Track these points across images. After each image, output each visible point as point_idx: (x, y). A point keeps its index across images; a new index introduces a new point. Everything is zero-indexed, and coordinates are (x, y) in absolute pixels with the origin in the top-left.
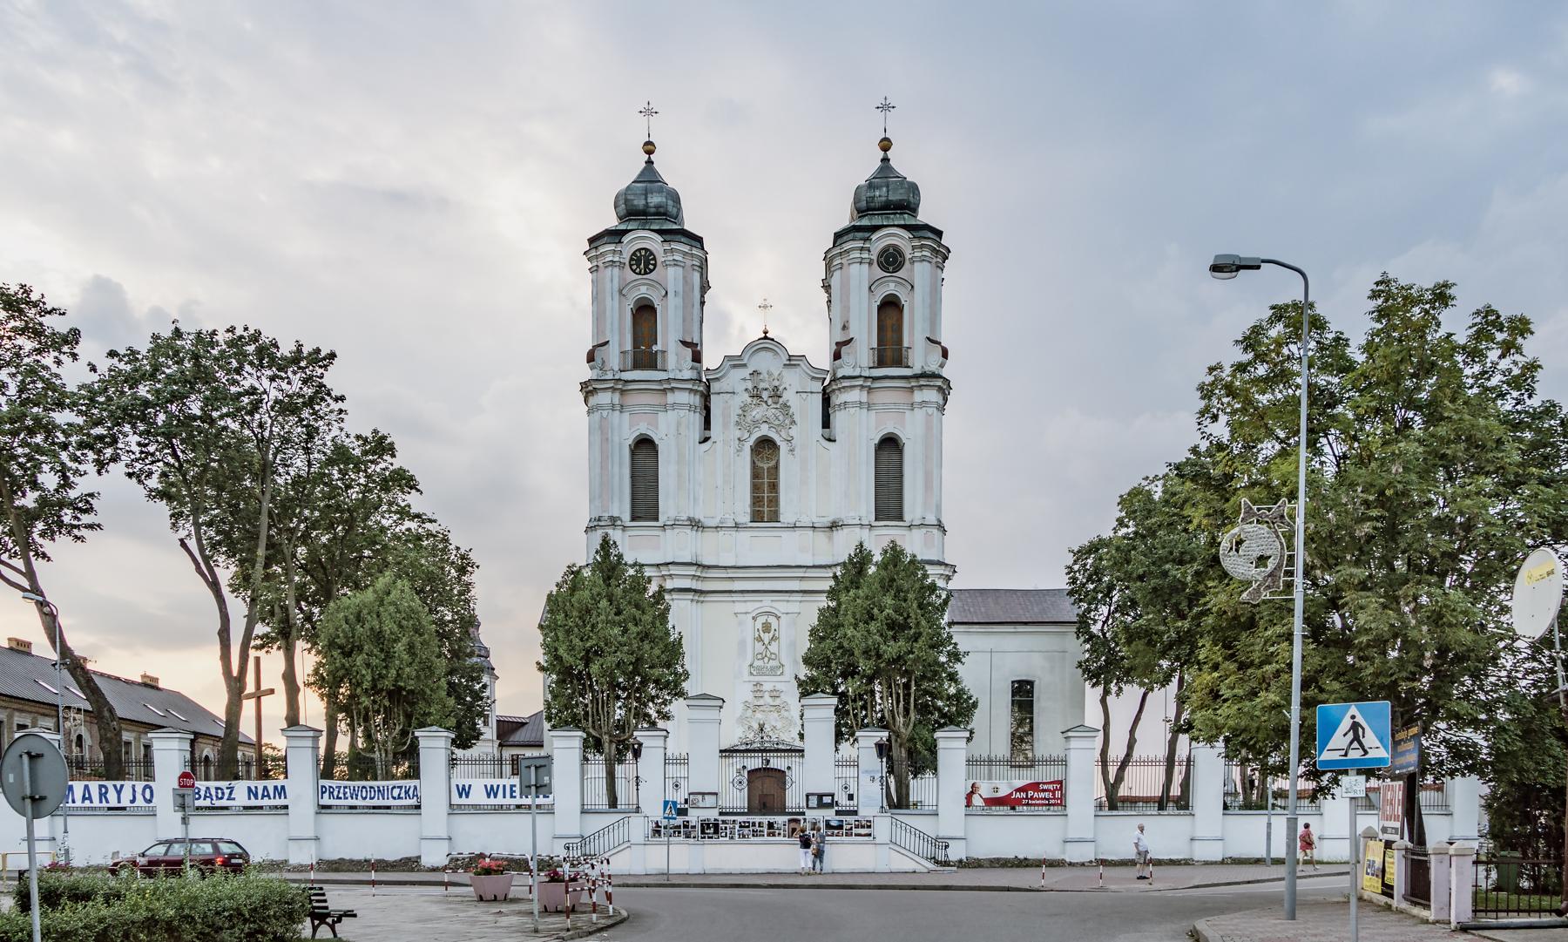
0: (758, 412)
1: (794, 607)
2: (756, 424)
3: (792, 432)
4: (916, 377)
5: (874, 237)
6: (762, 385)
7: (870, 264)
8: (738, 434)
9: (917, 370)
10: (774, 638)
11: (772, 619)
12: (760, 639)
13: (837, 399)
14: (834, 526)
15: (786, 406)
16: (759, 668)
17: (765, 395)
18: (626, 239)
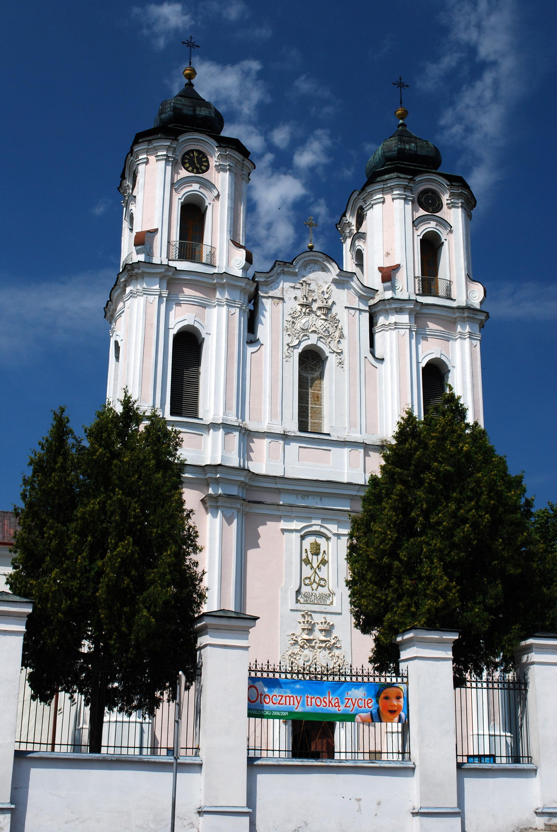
3: (340, 346)
4: (459, 308)
5: (418, 179)
7: (413, 202)
8: (287, 340)
10: (324, 562)
11: (321, 541)
12: (308, 562)
13: (381, 320)
16: (306, 596)
17: (315, 306)
18: (182, 138)
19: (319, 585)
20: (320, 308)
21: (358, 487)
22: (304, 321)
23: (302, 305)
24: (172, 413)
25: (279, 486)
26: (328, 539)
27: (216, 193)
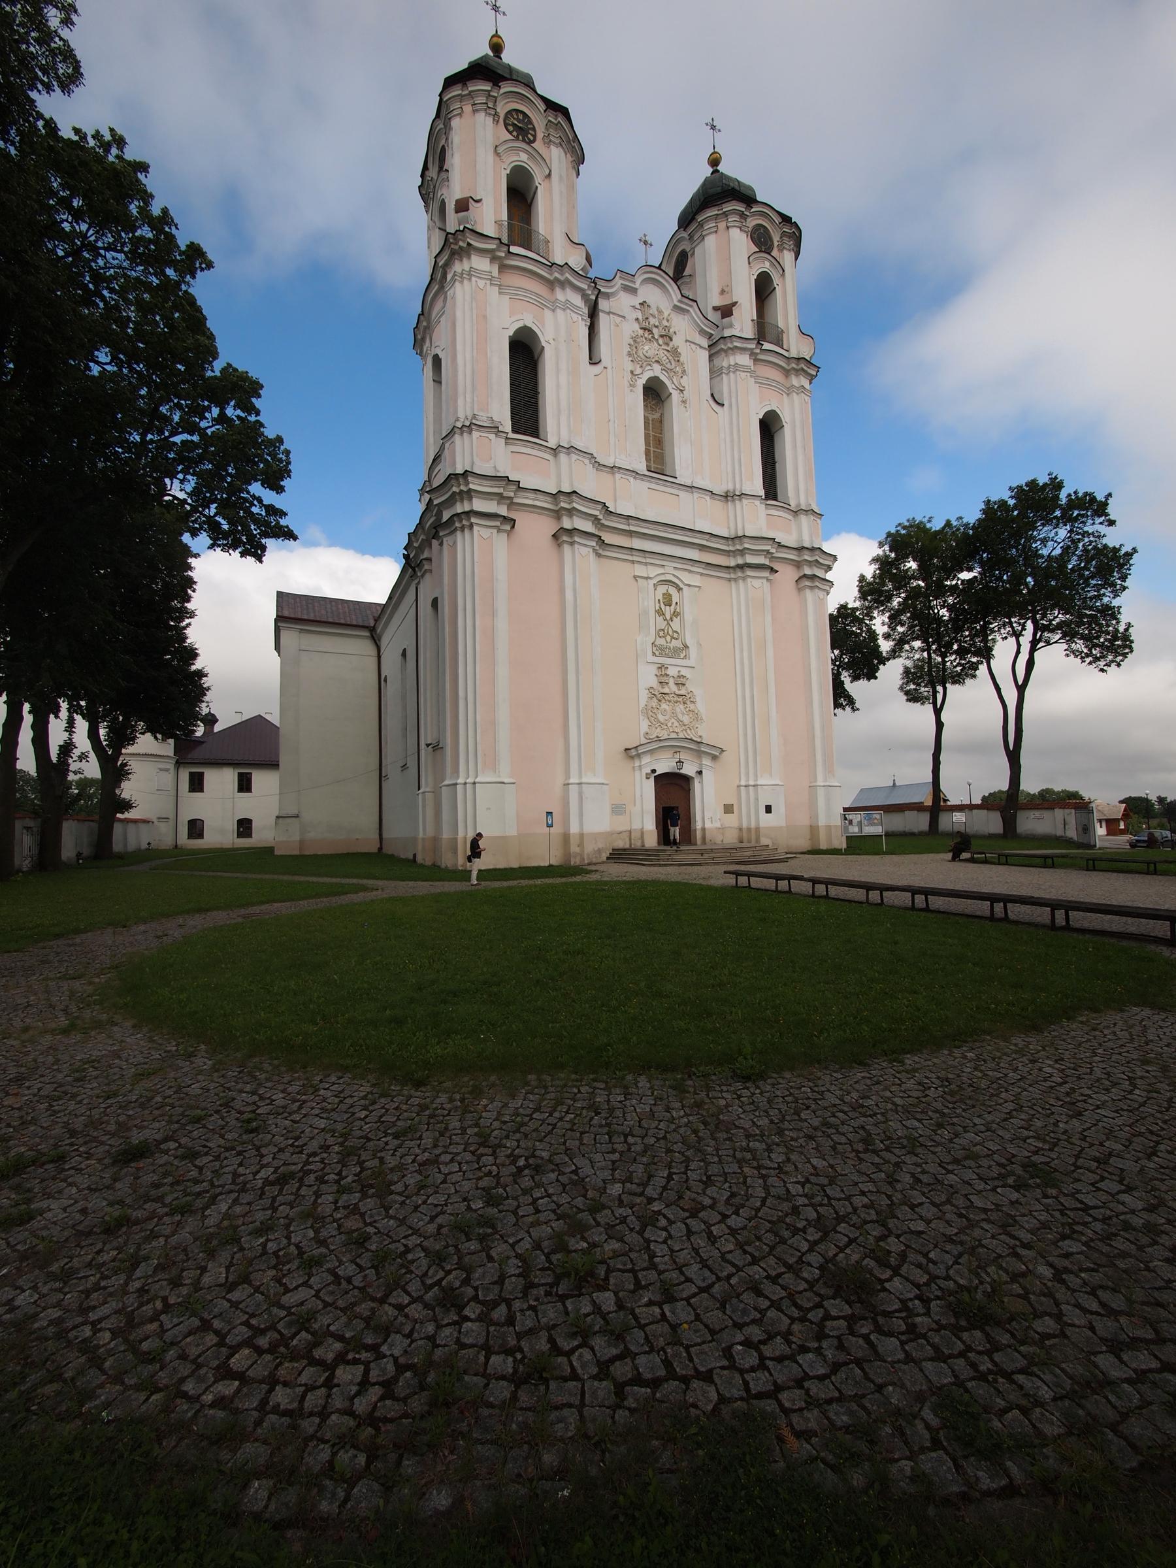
0: (649, 349)
1: (695, 580)
2: (648, 361)
6: (653, 321)
9: (794, 354)
10: (676, 614)
11: (672, 591)
12: (660, 613)
14: (728, 497)
15: (675, 353)
16: (661, 648)
19: (673, 638)
20: (662, 336)
21: (707, 537)
22: (646, 348)
23: (645, 329)
24: (514, 431)
25: (632, 528)
26: (680, 589)
27: (547, 172)
